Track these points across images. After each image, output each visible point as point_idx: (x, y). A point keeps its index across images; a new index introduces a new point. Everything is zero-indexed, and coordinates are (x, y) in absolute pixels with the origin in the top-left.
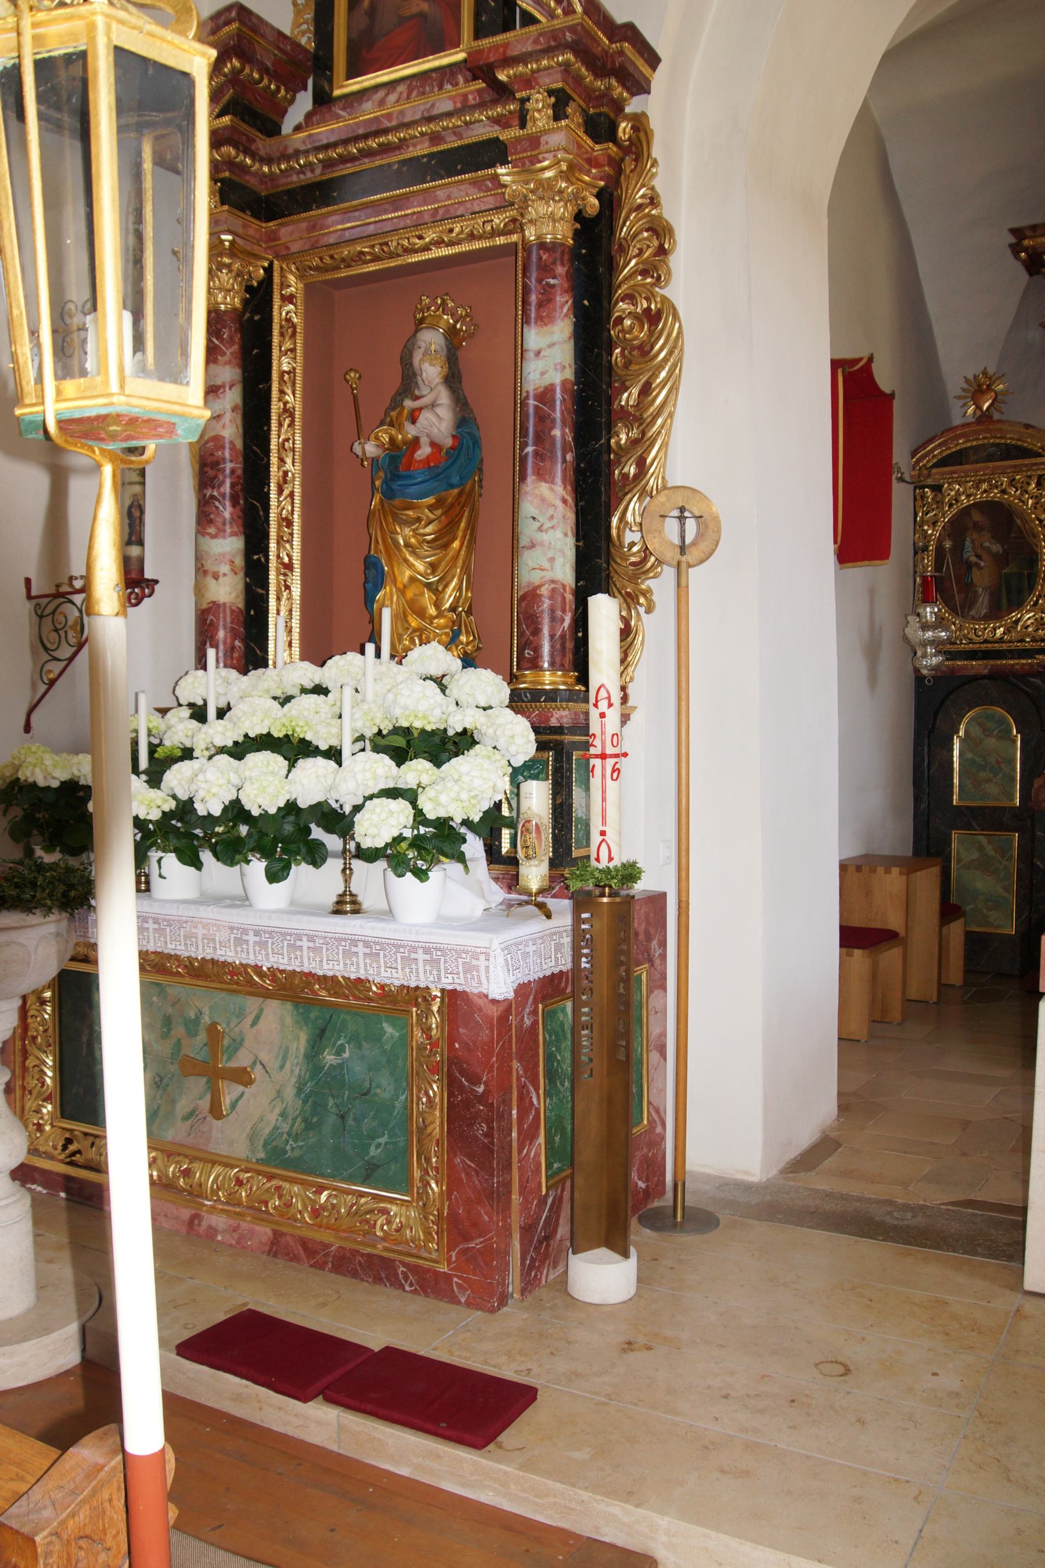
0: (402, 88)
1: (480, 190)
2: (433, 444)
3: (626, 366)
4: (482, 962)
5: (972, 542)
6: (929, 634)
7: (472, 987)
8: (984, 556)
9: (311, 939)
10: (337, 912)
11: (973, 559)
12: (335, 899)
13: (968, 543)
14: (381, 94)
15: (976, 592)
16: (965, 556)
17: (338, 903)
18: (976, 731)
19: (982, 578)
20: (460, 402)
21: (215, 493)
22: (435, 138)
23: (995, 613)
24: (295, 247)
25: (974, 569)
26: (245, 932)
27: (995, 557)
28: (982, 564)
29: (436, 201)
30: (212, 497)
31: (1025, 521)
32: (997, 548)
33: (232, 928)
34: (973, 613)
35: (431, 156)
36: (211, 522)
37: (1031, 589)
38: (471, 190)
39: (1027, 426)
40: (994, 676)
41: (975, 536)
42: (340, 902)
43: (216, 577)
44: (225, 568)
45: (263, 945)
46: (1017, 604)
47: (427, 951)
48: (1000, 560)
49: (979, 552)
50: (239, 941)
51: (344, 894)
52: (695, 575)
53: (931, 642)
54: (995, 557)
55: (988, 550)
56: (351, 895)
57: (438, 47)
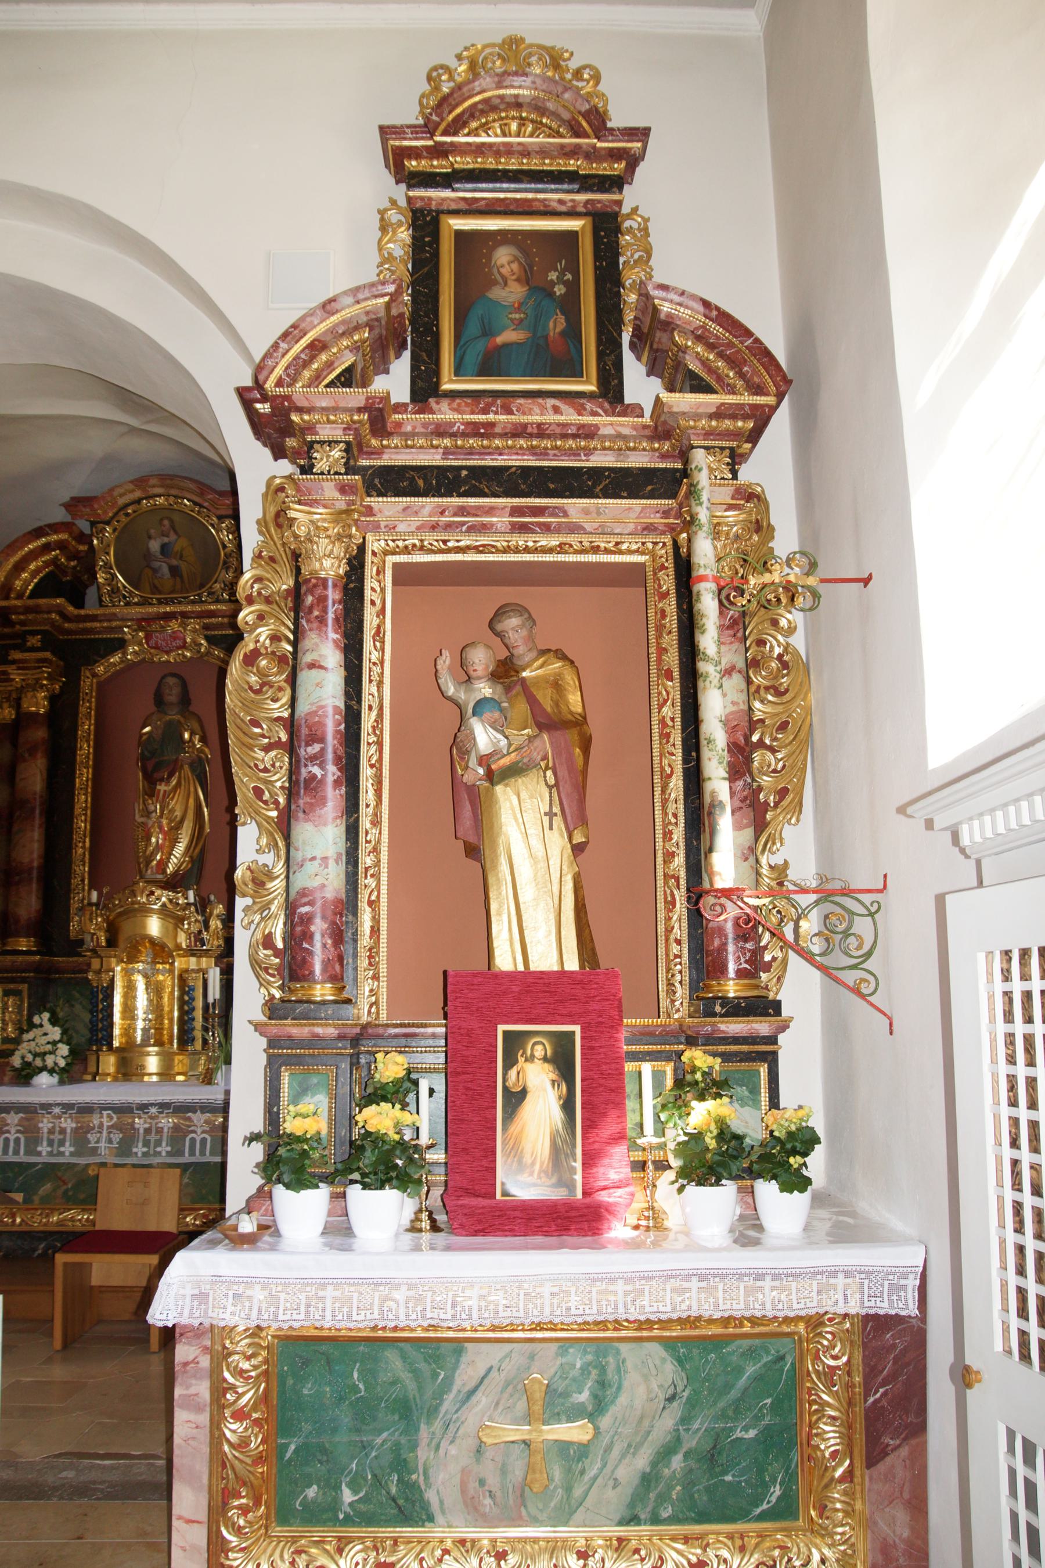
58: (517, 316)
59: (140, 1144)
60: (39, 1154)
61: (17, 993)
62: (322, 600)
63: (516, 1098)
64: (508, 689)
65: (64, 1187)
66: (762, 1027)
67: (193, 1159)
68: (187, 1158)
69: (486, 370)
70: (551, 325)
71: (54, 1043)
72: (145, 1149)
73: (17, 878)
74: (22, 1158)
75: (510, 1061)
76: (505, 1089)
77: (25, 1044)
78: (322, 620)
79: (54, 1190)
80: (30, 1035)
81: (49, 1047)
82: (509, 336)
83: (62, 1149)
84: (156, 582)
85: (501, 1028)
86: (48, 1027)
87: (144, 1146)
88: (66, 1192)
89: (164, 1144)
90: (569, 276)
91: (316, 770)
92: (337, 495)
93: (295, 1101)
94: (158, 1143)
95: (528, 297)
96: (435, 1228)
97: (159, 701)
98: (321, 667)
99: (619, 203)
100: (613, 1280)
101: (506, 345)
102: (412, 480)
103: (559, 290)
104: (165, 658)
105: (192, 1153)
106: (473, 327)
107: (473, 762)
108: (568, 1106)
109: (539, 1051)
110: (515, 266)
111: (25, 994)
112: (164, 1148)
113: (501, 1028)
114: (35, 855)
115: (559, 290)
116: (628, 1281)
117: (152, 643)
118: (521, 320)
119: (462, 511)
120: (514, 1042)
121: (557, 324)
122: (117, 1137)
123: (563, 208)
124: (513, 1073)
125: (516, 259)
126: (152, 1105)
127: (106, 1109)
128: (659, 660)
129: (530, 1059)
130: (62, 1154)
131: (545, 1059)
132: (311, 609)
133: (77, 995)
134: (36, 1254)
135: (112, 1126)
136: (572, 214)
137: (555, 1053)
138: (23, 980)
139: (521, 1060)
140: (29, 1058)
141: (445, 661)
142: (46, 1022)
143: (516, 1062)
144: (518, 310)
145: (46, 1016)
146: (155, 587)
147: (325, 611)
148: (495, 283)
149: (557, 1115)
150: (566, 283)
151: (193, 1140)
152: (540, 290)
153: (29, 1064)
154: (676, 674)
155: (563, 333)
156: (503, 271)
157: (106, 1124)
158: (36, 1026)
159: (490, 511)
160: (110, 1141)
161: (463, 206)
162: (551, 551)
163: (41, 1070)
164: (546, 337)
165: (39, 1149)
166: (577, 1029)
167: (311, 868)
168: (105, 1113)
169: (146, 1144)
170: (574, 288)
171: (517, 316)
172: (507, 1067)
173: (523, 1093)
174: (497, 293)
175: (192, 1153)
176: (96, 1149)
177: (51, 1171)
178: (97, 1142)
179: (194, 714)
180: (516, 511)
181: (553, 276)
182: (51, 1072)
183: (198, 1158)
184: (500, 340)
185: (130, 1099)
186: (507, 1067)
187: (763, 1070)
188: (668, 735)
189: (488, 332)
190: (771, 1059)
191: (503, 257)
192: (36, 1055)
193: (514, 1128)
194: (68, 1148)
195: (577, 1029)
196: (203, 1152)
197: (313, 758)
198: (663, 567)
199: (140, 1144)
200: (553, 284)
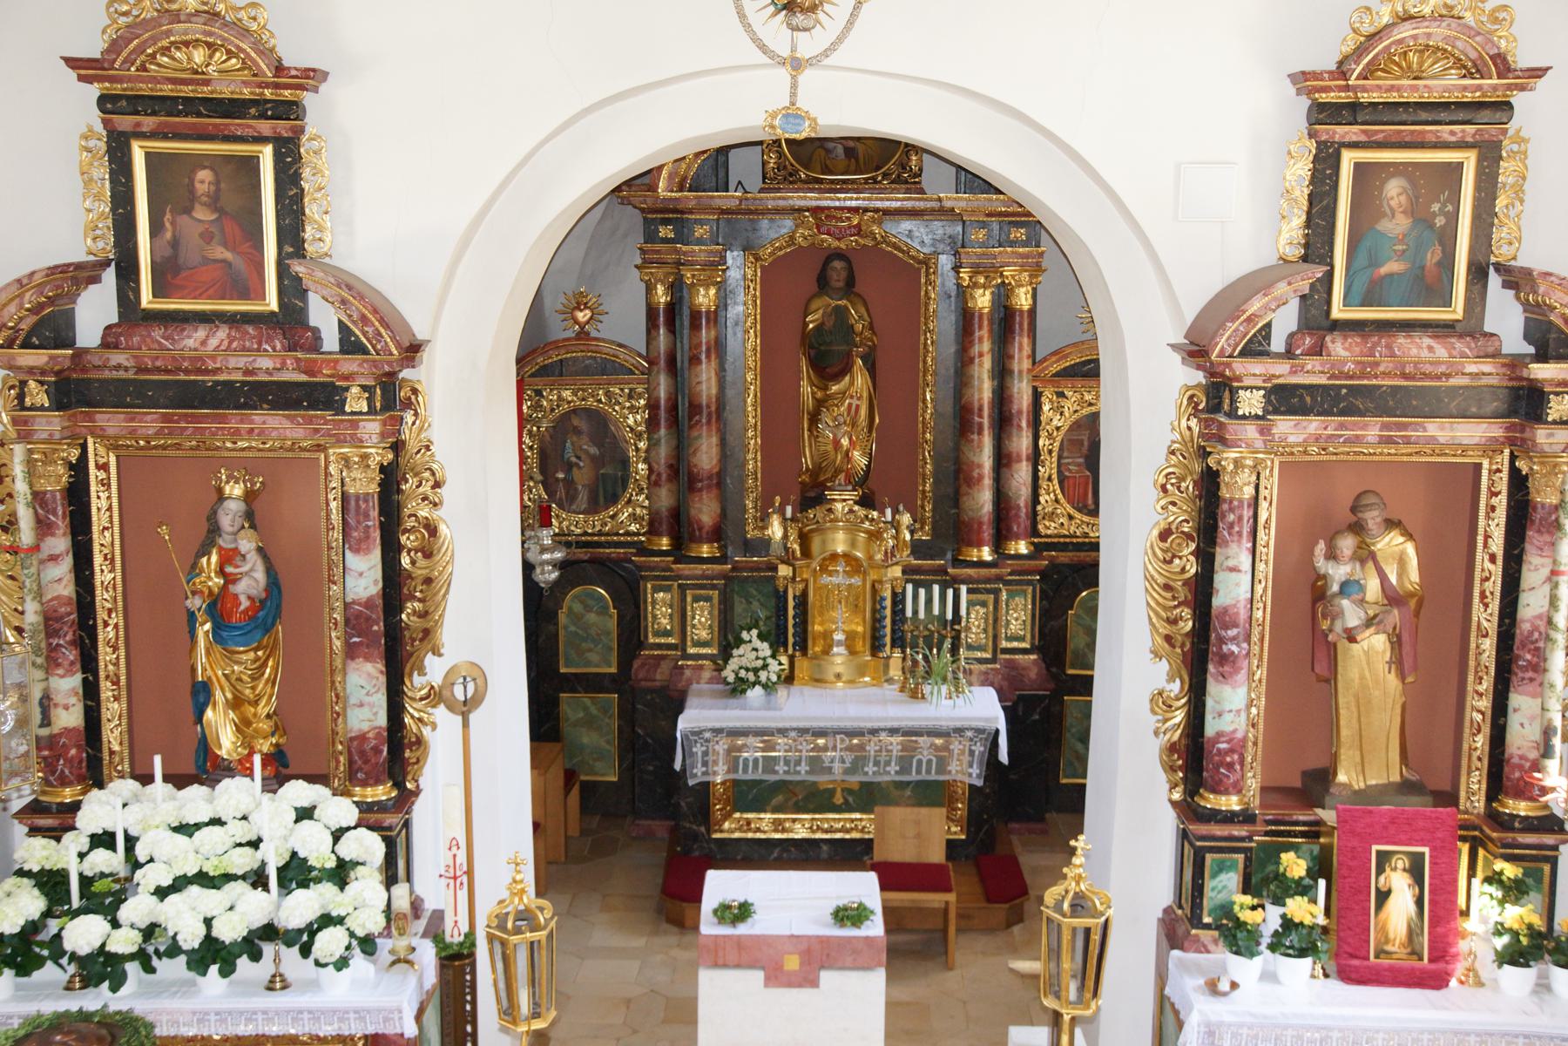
0: (222, 333)
1: (292, 422)
2: (249, 598)
3: (413, 562)
4: (396, 1016)
5: (572, 444)
6: (546, 556)
7: (390, 1030)
8: (583, 456)
9: (265, 1012)
10: (270, 989)
11: (574, 459)
12: (269, 978)
13: (568, 445)
14: (201, 333)
15: (576, 489)
16: (566, 457)
17: (271, 982)
18: (578, 607)
19: (583, 476)
20: (270, 570)
21: (62, 642)
22: (247, 372)
23: (593, 508)
24: (110, 432)
25: (575, 469)
26: (207, 1013)
27: (593, 458)
28: (582, 464)
29: (252, 422)
30: (58, 645)
31: (618, 428)
32: (594, 450)
33: (194, 1013)
34: (574, 507)
35: (244, 383)
36: (58, 665)
37: (625, 488)
38: (284, 421)
39: (621, 345)
40: (592, 561)
41: (575, 439)
42: (272, 981)
43: (66, 708)
44: (73, 700)
45: (223, 1021)
46: (613, 499)
47: (356, 1012)
48: (597, 462)
49: (578, 453)
50: (200, 1021)
51: (274, 976)
52: (473, 717)
53: (548, 562)
54: (593, 458)
55: (586, 452)
56: (281, 975)
57: (244, 295)
58: (1400, 247)
59: (871, 764)
60: (776, 772)
61: (708, 599)
62: (1240, 518)
63: (1384, 896)
64: (1363, 562)
65: (794, 799)
66: (1549, 839)
67: (919, 778)
68: (914, 777)
69: (1367, 302)
70: (1429, 255)
71: (764, 659)
72: (875, 769)
73: (700, 485)
74: (759, 776)
75: (1380, 870)
76: (1377, 889)
77: (735, 660)
78: (1240, 534)
79: (786, 801)
80: (741, 651)
81: (760, 663)
82: (1392, 267)
83: (798, 768)
84: (828, 162)
85: (1375, 848)
86: (757, 643)
87: (875, 765)
88: (796, 804)
89: (893, 764)
90: (1450, 208)
91: (1234, 648)
92: (1257, 435)
93: (1214, 876)
94: (888, 763)
95: (1412, 229)
96: (1326, 976)
97: (823, 283)
98: (1239, 571)
99: (1505, 132)
100: (1468, 1034)
101: (1390, 275)
102: (1301, 396)
103: (1440, 221)
104: (836, 244)
105: (919, 772)
106: (1362, 259)
107: (1338, 627)
108: (1419, 902)
109: (1400, 864)
110: (1403, 198)
111: (716, 601)
112: (893, 768)
113: (1375, 848)
114: (714, 462)
115: (1440, 221)
116: (1478, 1035)
117: (824, 229)
118: (1404, 251)
119: (1342, 426)
120: (1383, 858)
121: (1433, 256)
122: (849, 757)
123: (1453, 139)
124: (1382, 879)
125: (1405, 191)
126: (882, 730)
127: (839, 733)
128: (1486, 545)
129: (1395, 869)
130: (799, 773)
131: (1404, 870)
132: (1231, 526)
133: (755, 593)
134: (772, 857)
135: (847, 749)
136: (1461, 145)
137: (1411, 865)
138: (714, 587)
139: (1388, 869)
140: (743, 673)
141: (1321, 547)
142: (755, 638)
143: (1384, 871)
144: (1401, 242)
145: (755, 632)
146: (826, 166)
147: (1241, 527)
148: (1384, 215)
149: (1412, 908)
150: (1446, 214)
151: (920, 762)
152: (1422, 220)
153: (742, 680)
154: (1500, 561)
155: (1439, 264)
156: (1393, 203)
157: (839, 746)
158: (746, 642)
159: (1365, 427)
160: (843, 761)
161: (1363, 138)
162: (1411, 455)
163: (754, 684)
164: (1423, 268)
165: (777, 768)
166: (1426, 850)
167: (1228, 717)
168: (838, 737)
169: (876, 763)
170: (1454, 218)
171: (1400, 247)
172: (1379, 873)
173: (1389, 892)
174: (1385, 226)
175: (919, 772)
176: (830, 768)
177: (781, 786)
178: (832, 762)
179: (859, 296)
180: (1385, 427)
181: (1436, 207)
182: (765, 686)
183: (924, 776)
184: (1383, 270)
185: (862, 725)
186: (1379, 873)
187: (1547, 868)
188: (1486, 606)
189: (1374, 263)
190: (1554, 862)
191: (1394, 190)
192: (747, 670)
193: (1382, 915)
194: (803, 768)
195: (1426, 850)
196: (928, 772)
197: (1233, 639)
198: (1499, 471)
199: (871, 764)
200: (1434, 215)
